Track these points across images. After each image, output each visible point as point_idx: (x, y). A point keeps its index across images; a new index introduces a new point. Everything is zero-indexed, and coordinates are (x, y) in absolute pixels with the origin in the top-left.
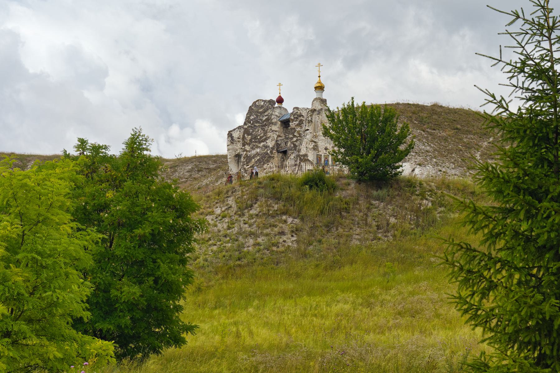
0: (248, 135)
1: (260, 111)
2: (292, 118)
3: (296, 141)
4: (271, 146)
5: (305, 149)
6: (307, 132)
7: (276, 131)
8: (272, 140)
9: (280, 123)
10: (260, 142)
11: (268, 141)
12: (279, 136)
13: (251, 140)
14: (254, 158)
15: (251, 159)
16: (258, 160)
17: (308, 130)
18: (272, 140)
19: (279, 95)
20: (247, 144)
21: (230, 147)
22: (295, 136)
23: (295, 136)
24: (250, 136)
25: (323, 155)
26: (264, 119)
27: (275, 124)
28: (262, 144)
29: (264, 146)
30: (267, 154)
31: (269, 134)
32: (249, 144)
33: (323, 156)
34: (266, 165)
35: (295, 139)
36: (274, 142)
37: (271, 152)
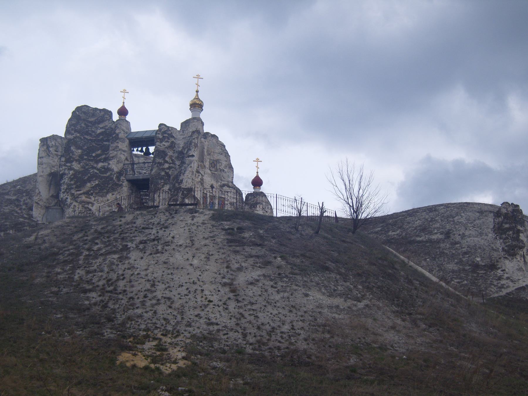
0: (78, 148)
1: (90, 120)
2: (160, 136)
3: (169, 168)
4: (116, 169)
5: (190, 181)
6: (191, 158)
7: (124, 151)
8: (118, 162)
9: (128, 141)
10: (97, 162)
11: (111, 162)
12: (127, 159)
13: (81, 156)
14: (90, 182)
15: (86, 183)
16: (97, 185)
17: (193, 156)
18: (118, 162)
19: (121, 105)
20: (76, 161)
21: (45, 160)
22: (167, 162)
23: (167, 162)
24: (80, 151)
25: (208, 194)
26: (99, 131)
27: (123, 141)
28: (100, 165)
29: (103, 167)
30: (112, 179)
31: (112, 153)
32: (79, 161)
33: (208, 196)
34: (110, 194)
35: (166, 166)
36: (121, 165)
37: (118, 178)
